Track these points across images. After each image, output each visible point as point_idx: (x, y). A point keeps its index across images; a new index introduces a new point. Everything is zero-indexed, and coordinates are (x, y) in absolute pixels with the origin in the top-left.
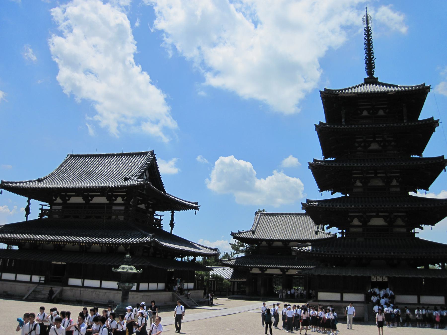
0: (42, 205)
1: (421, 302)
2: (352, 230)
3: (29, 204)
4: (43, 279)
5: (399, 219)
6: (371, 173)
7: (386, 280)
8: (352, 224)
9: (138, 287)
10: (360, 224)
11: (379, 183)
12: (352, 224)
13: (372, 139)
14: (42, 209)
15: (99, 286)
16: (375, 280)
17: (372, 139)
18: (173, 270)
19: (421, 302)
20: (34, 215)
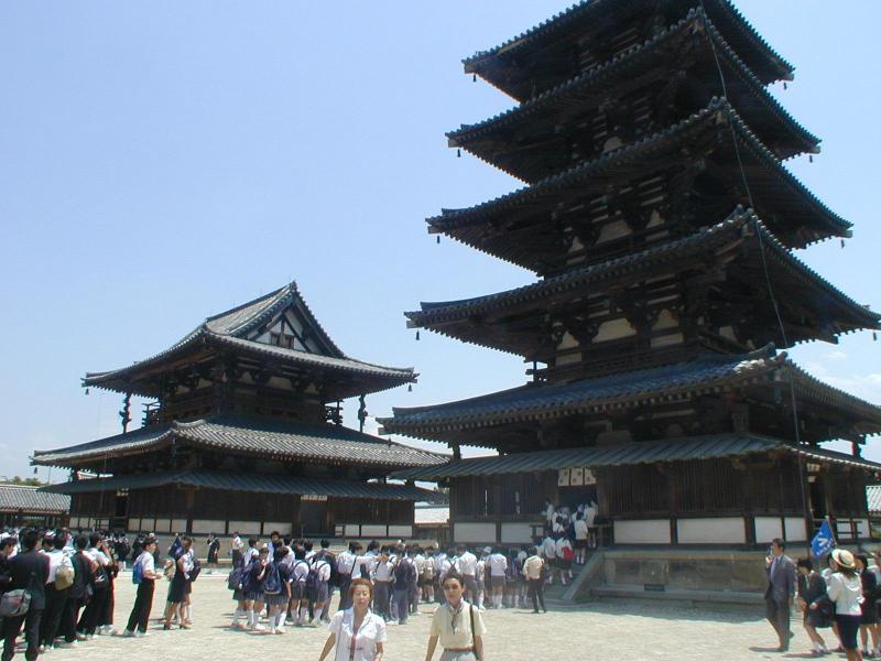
0: (148, 406)
1: (680, 541)
2: (562, 361)
3: (128, 405)
4: (105, 523)
5: (665, 312)
6: (602, 213)
7: (593, 481)
8: (561, 347)
9: (189, 527)
10: (576, 344)
11: (620, 230)
12: (561, 347)
13: (605, 133)
14: (147, 412)
15: (385, 534)
16: (565, 483)
17: (605, 133)
18: (325, 498)
19: (680, 541)
20: (136, 423)
